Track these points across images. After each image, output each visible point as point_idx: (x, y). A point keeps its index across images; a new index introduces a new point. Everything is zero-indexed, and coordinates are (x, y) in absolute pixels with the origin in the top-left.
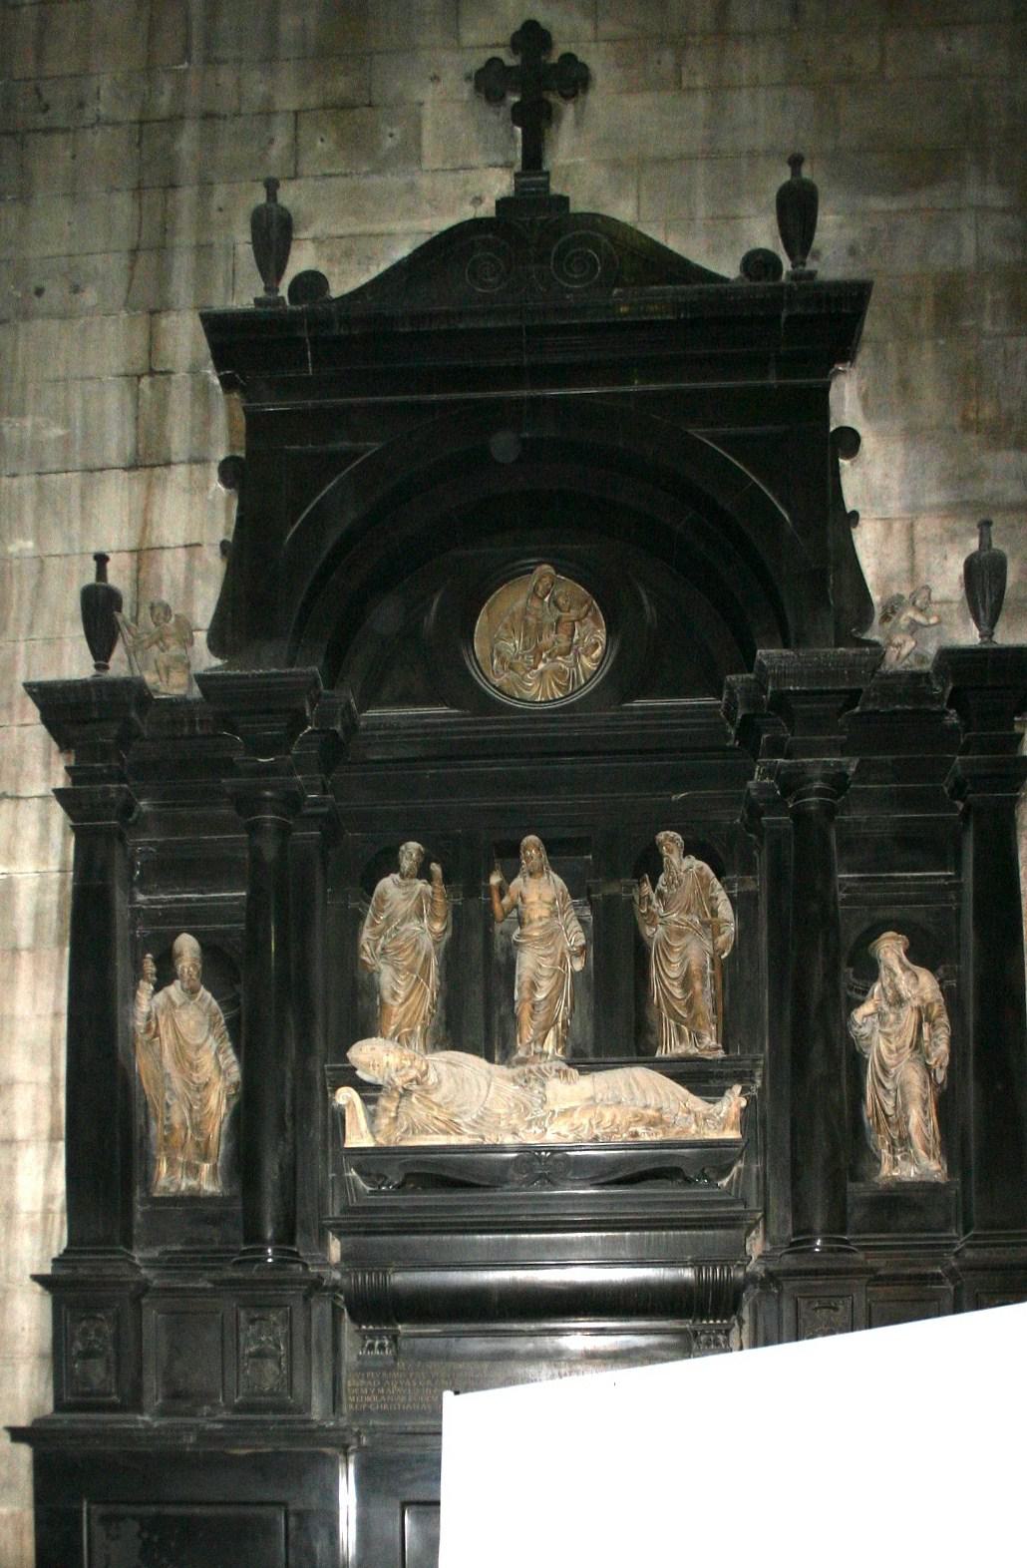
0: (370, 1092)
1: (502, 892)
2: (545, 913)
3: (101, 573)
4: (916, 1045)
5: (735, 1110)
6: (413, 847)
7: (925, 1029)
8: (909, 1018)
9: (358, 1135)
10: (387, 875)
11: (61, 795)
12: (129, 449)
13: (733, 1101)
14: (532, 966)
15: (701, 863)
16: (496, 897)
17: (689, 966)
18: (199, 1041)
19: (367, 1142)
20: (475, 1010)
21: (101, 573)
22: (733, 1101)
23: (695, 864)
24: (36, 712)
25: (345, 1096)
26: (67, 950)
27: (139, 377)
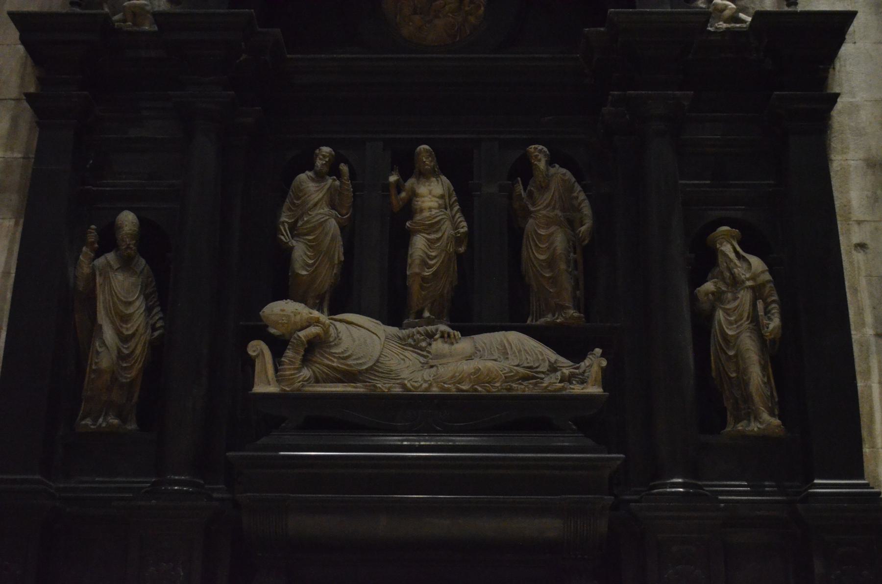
0: (278, 346)
1: (399, 188)
2: (434, 204)
4: (754, 318)
5: (595, 368)
6: (326, 150)
7: (760, 305)
8: (745, 297)
9: (265, 384)
10: (303, 172)
11: (29, 97)
13: (595, 362)
14: (423, 247)
15: (564, 171)
16: (393, 191)
17: (555, 249)
18: (131, 300)
19: (273, 389)
20: (373, 280)
22: (595, 362)
23: (560, 172)
24: (17, 34)
25: (257, 348)
26: (22, 221)
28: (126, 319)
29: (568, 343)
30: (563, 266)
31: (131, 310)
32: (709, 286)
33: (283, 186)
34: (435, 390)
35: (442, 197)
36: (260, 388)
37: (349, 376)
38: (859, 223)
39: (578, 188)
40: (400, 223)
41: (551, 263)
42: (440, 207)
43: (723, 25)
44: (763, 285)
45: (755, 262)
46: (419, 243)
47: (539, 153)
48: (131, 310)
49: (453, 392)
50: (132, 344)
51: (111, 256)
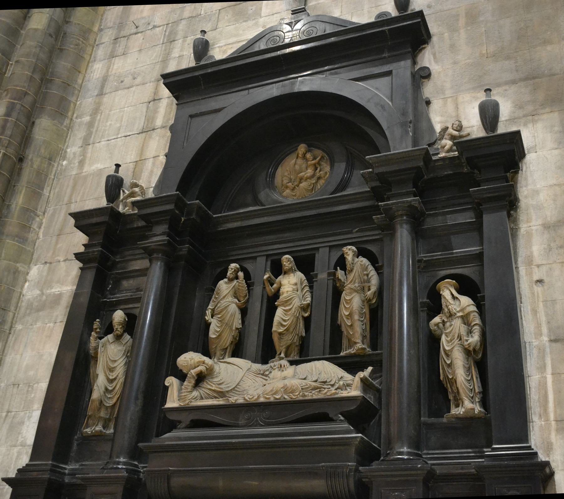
3: (117, 171)
6: (233, 266)
12: (141, 127)
16: (267, 284)
17: (353, 308)
21: (117, 171)
23: (364, 261)
27: (149, 102)
28: (112, 370)
29: (351, 365)
30: (356, 317)
31: (115, 365)
32: (437, 319)
33: (211, 290)
34: (262, 400)
35: (296, 284)
36: (169, 405)
37: (222, 394)
38: (538, 266)
39: (371, 268)
40: (271, 302)
41: (350, 316)
42: (294, 290)
43: (442, 155)
44: (468, 314)
45: (465, 300)
46: (279, 313)
47: (349, 252)
48: (115, 365)
49: (272, 399)
50: (114, 384)
51: (110, 337)
